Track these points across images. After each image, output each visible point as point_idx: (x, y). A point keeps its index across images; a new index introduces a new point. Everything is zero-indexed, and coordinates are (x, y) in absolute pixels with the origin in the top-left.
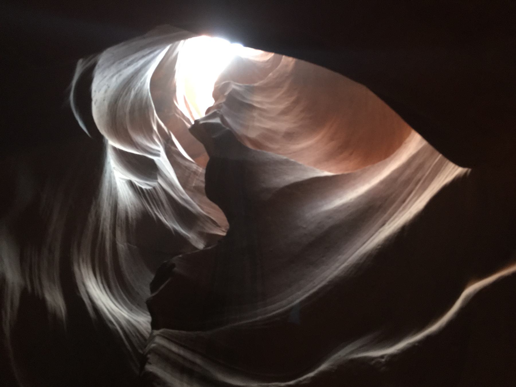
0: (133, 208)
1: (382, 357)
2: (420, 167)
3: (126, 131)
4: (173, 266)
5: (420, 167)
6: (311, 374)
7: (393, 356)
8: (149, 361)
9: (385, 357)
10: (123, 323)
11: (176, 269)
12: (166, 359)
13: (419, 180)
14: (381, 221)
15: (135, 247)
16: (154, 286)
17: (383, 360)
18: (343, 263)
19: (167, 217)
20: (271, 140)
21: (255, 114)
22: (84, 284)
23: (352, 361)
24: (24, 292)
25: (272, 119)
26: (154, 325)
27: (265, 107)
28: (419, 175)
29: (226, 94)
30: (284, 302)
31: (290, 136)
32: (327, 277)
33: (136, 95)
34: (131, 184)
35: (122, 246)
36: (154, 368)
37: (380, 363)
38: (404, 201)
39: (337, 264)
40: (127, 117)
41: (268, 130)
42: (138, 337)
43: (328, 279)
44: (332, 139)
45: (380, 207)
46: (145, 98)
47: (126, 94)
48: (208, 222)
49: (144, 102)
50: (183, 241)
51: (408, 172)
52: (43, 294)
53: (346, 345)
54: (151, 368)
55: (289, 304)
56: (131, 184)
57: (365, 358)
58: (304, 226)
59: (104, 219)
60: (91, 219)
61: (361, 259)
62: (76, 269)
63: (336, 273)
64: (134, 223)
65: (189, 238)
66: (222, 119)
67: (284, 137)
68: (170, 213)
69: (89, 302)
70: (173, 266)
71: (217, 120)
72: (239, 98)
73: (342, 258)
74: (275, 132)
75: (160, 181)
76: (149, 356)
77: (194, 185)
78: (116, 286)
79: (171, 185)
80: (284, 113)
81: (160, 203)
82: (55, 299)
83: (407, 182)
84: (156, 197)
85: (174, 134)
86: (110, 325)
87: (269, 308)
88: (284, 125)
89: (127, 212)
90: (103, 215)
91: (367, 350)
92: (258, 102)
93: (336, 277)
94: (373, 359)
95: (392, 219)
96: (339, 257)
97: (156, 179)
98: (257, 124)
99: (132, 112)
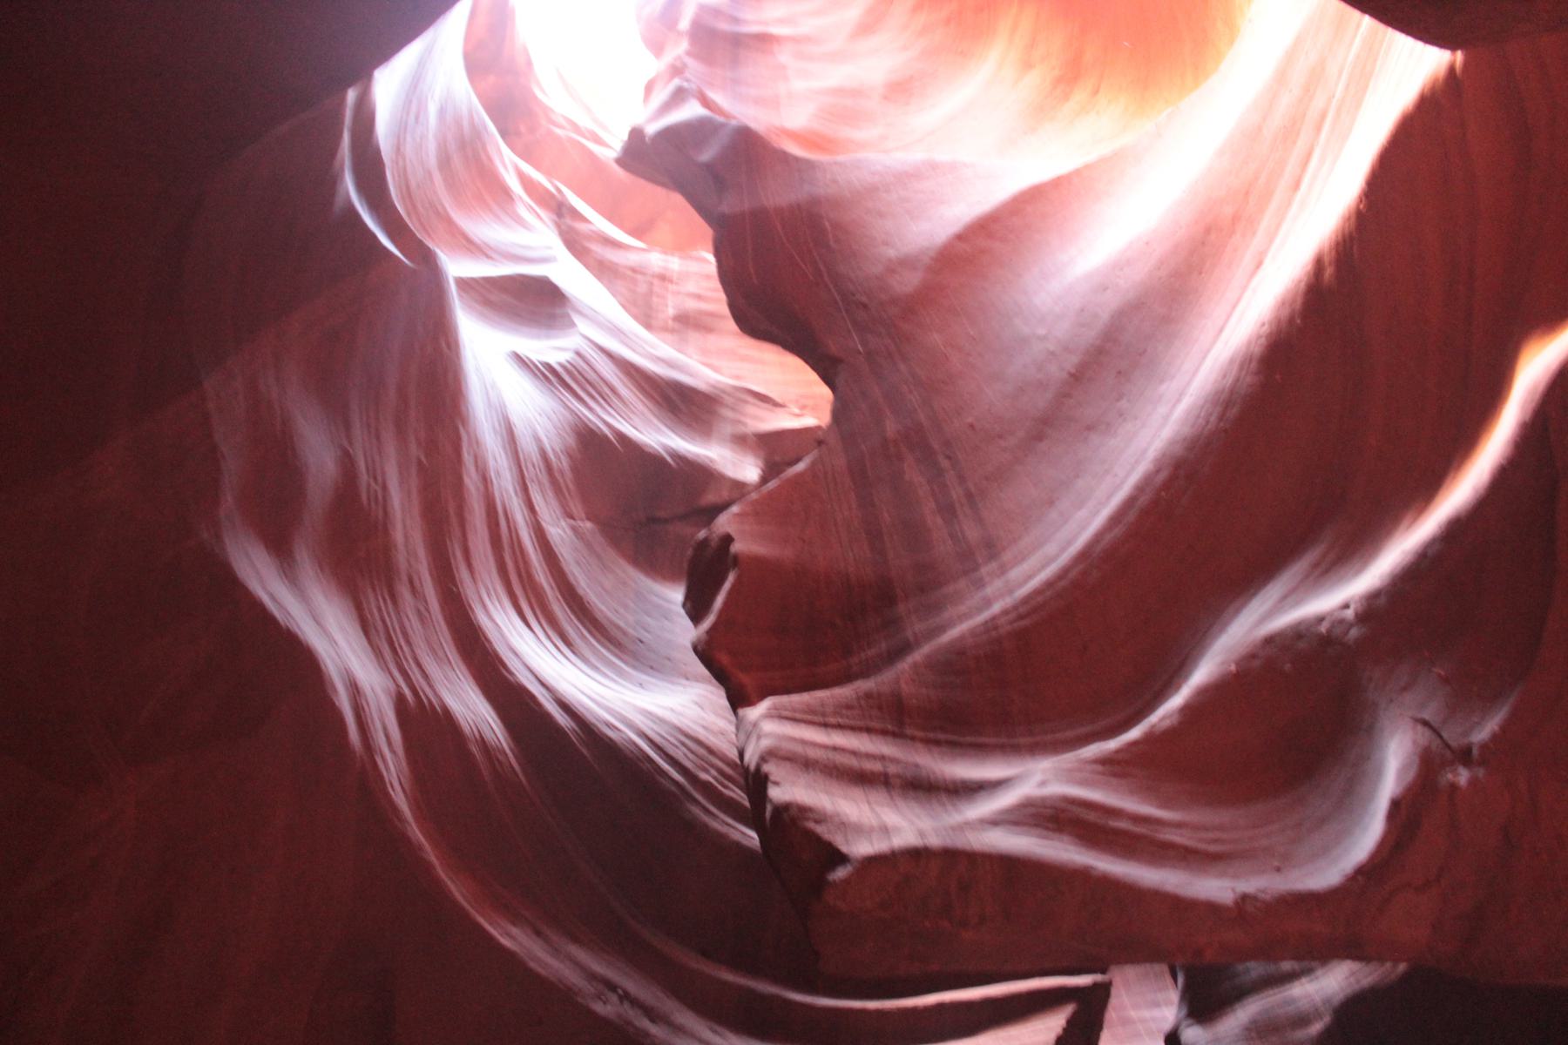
0: (550, 427)
1: (1346, 606)
2: (1316, 77)
3: (449, 222)
4: (728, 539)
5: (1316, 77)
7: (1372, 597)
8: (772, 778)
9: (1352, 607)
10: (639, 721)
11: (736, 547)
12: (805, 764)
13: (1323, 116)
14: (1248, 259)
15: (589, 525)
16: (696, 608)
18: (1178, 401)
19: (636, 420)
20: (852, 116)
21: (784, 56)
22: (516, 654)
23: (1269, 640)
24: (400, 703)
25: (836, 57)
26: (738, 699)
27: (806, 27)
28: (1318, 103)
29: (684, 24)
30: (1050, 549)
31: (901, 90)
32: (1145, 451)
33: (442, 112)
34: (521, 361)
35: (558, 532)
36: (787, 790)
37: (1342, 621)
38: (1297, 185)
39: (1162, 410)
40: (438, 178)
41: (839, 92)
42: (683, 744)
44: (1027, 65)
45: (1236, 218)
46: (465, 112)
47: (417, 118)
48: (746, 402)
49: (465, 123)
50: (697, 475)
51: (1286, 101)
53: (1243, 605)
54: (776, 794)
56: (521, 361)
58: (1041, 331)
59: (498, 473)
60: (471, 481)
61: (1224, 376)
62: (482, 619)
64: (565, 463)
65: (712, 461)
66: (706, 102)
67: (886, 98)
68: (641, 407)
69: (544, 691)
70: (728, 539)
71: (691, 111)
72: (724, 26)
73: (1169, 388)
74: (856, 93)
75: (583, 326)
76: (766, 768)
77: (671, 312)
78: (583, 637)
79: (616, 332)
80: (866, 27)
81: (606, 390)
83: (1290, 132)
84: (592, 376)
85: (570, 187)
87: (1015, 574)
88: (877, 63)
89: (538, 440)
90: (491, 463)
91: (1298, 603)
92: (781, 21)
93: (1172, 442)
94: (1320, 619)
95: (1278, 241)
96: (1163, 387)
97: (573, 325)
98: (798, 85)
99: (445, 162)
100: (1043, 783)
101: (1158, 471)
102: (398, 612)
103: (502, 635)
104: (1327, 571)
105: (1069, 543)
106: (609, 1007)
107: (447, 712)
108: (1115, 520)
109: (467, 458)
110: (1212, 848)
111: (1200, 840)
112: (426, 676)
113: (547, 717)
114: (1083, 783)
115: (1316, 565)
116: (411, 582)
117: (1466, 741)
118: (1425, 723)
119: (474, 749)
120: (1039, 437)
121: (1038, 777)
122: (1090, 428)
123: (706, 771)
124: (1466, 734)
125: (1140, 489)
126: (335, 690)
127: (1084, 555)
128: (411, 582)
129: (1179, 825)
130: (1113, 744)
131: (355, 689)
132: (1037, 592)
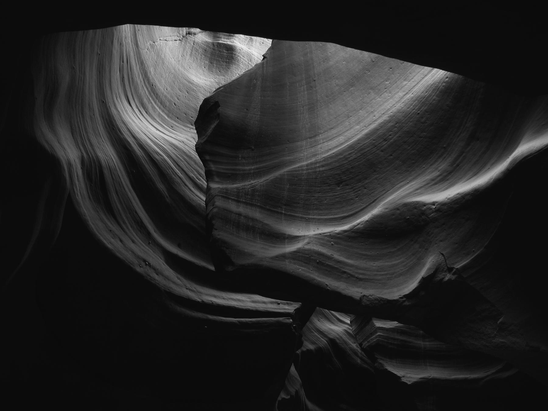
1: (433, 204)
6: (366, 217)
17: (434, 207)
23: (406, 205)
37: (431, 209)
39: (401, 94)
43: (390, 113)
52: (95, 153)
55: (346, 141)
57: (418, 203)
63: (399, 106)
76: (214, 222)
82: (107, 153)
86: (157, 157)
91: (421, 194)
93: (399, 111)
94: (424, 204)
96: (405, 83)
100: (308, 243)
101: (389, 121)
102: (83, 117)
103: (121, 117)
104: (436, 184)
105: (349, 139)
106: (142, 268)
107: (97, 157)
108: (368, 136)
109: (115, 42)
110: (361, 276)
111: (357, 273)
112: (91, 145)
113: (134, 151)
114: (323, 245)
115: (433, 180)
116: (89, 105)
117: (452, 266)
118: (442, 254)
119: (106, 172)
120: (352, 85)
121: (306, 241)
122: (372, 88)
123: (192, 172)
124: (453, 264)
125: (382, 126)
126: (64, 170)
127: (351, 147)
128: (89, 105)
129: (352, 266)
130: (339, 229)
131: (70, 164)
132: (331, 157)
